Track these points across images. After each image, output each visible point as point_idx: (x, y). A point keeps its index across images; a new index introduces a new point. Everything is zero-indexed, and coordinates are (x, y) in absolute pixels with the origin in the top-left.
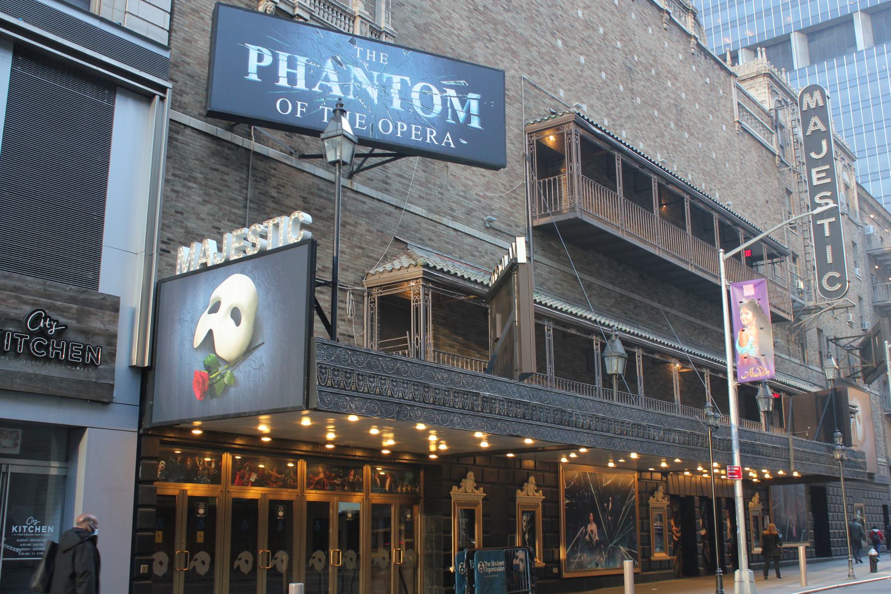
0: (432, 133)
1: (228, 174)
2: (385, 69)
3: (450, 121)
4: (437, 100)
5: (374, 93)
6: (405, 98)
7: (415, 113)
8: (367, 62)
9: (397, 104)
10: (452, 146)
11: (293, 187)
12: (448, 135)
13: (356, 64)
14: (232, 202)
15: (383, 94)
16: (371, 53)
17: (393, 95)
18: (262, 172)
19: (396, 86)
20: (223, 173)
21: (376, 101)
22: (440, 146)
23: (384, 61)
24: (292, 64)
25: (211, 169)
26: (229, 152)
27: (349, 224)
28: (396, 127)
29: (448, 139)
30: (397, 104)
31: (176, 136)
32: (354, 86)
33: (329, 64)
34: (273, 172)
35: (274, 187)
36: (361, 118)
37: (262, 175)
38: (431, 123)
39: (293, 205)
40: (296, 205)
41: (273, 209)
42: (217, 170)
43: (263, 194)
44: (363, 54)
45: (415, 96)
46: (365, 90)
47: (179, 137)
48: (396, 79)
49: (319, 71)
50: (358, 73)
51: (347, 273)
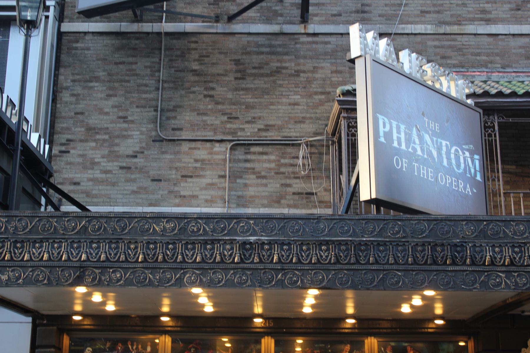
1: (136, 63)
11: (220, 53)
14: (143, 88)
18: (177, 49)
20: (131, 63)
25: (116, 64)
26: (137, 42)
27: (304, 72)
31: (75, 45)
34: (193, 46)
35: (195, 60)
37: (179, 53)
39: (221, 72)
40: (226, 71)
41: (195, 82)
42: (123, 63)
43: (180, 71)
47: (79, 45)
51: (302, 126)
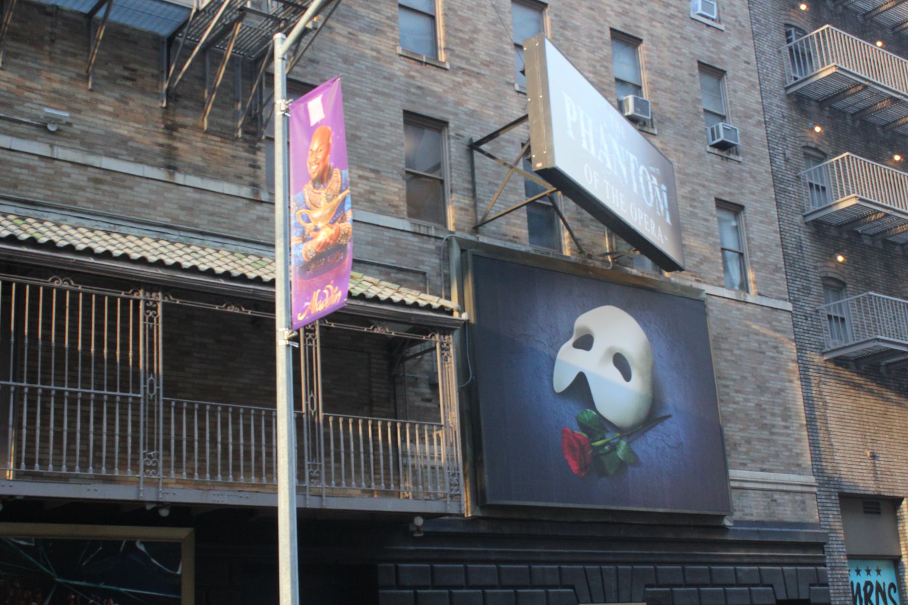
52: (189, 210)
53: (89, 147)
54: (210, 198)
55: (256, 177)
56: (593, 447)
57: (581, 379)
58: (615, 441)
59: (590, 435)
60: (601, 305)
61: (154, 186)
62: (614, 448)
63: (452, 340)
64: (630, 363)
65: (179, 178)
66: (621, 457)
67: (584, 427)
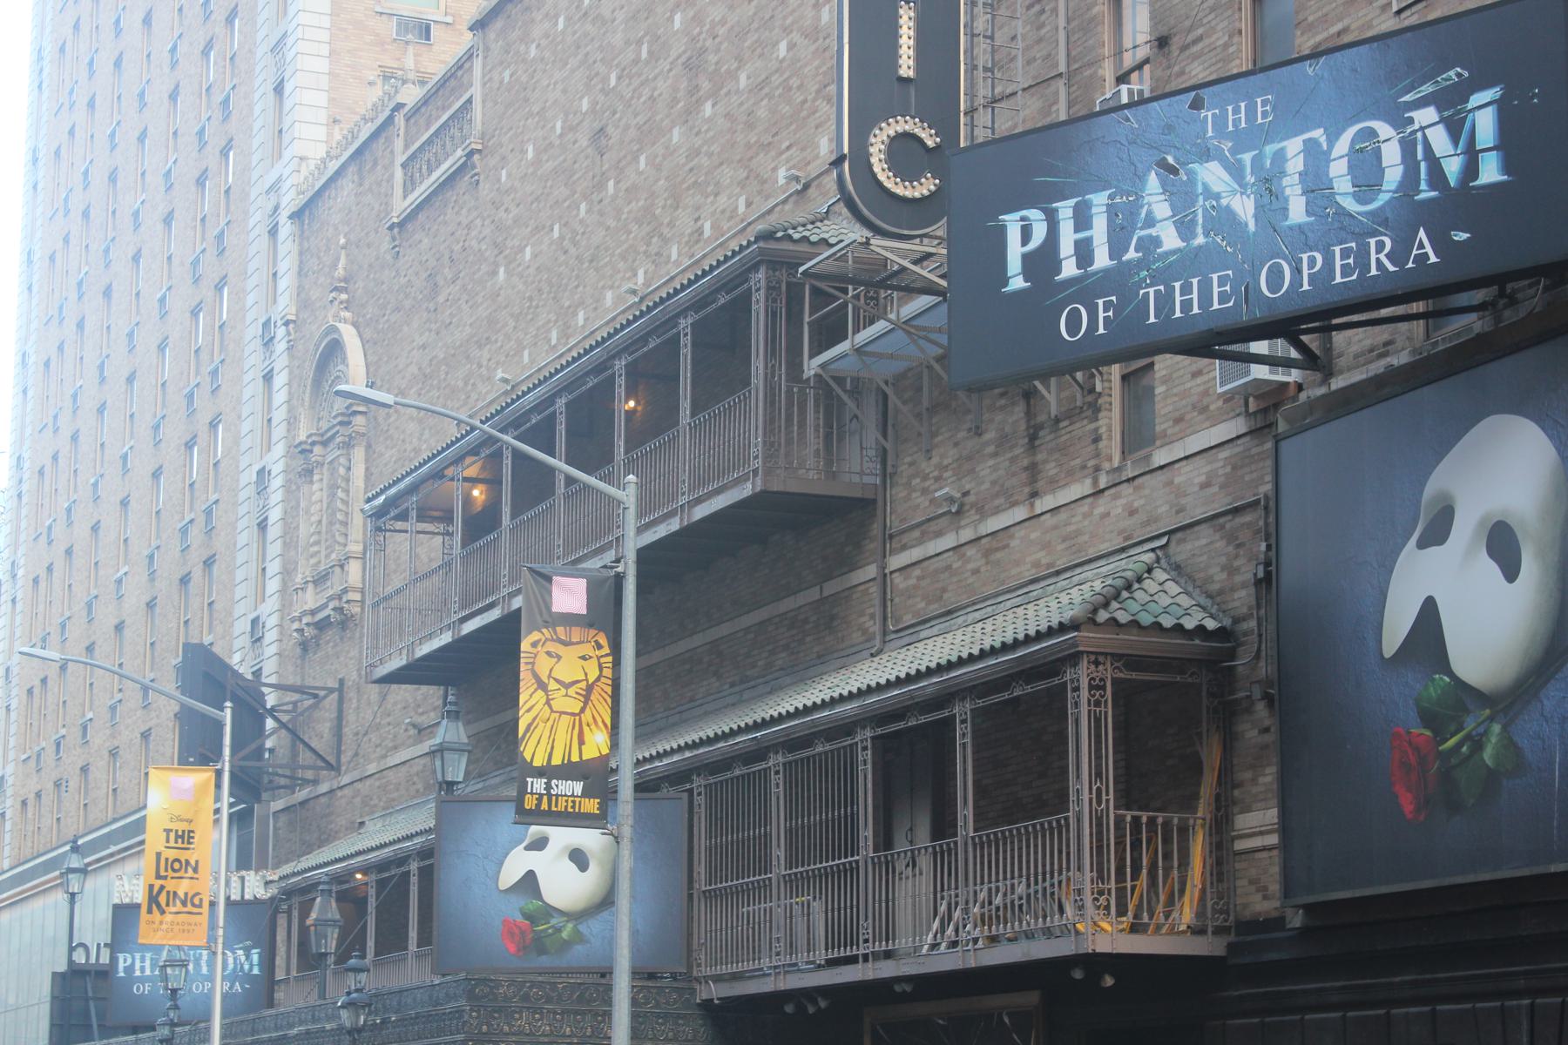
0: (1380, 246)
2: (1269, 134)
3: (1426, 193)
4: (1391, 154)
5: (1244, 208)
6: (1316, 186)
7: (1342, 212)
8: (1229, 136)
9: (1297, 211)
10: (1433, 259)
12: (1422, 234)
13: (1206, 155)
15: (1266, 200)
16: (1236, 111)
17: (1288, 191)
19: (1295, 164)
21: (1252, 227)
22: (1404, 271)
23: (1265, 114)
24: (1082, 220)
28: (1297, 271)
29: (1421, 246)
30: (1297, 211)
32: (1205, 210)
33: (1153, 181)
36: (1221, 283)
38: (1380, 220)
44: (1220, 122)
45: (1338, 169)
46: (1228, 210)
48: (1294, 146)
49: (1133, 210)
50: (1212, 175)
52: (1046, 546)
53: (983, 512)
54: (1063, 516)
55: (1097, 455)
56: (1440, 753)
57: (1429, 611)
58: (1481, 730)
59: (1436, 732)
60: (1467, 430)
61: (1020, 532)
62: (1477, 744)
63: (1083, 673)
64: (1520, 537)
65: (1041, 505)
66: (1489, 762)
67: (1429, 718)
